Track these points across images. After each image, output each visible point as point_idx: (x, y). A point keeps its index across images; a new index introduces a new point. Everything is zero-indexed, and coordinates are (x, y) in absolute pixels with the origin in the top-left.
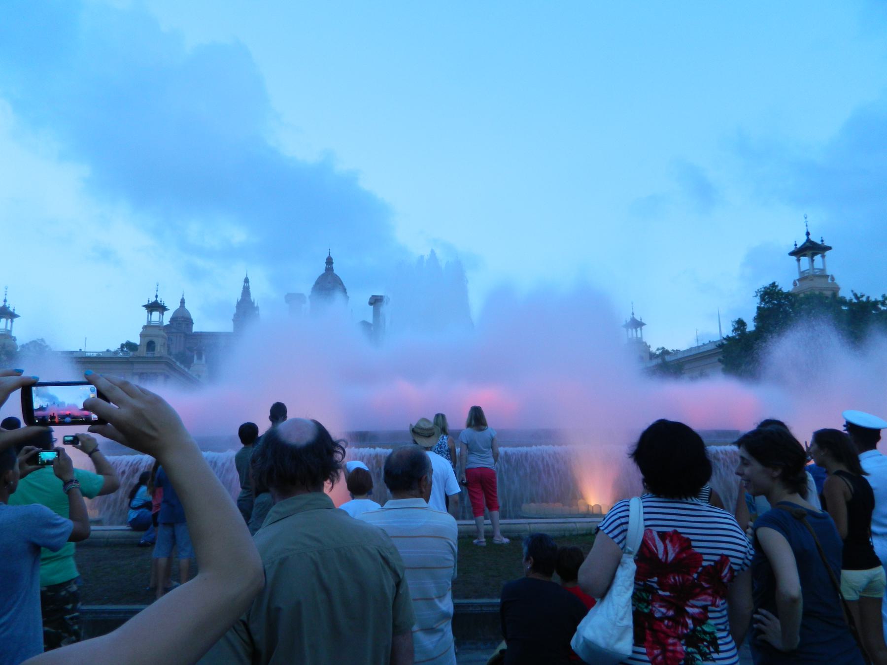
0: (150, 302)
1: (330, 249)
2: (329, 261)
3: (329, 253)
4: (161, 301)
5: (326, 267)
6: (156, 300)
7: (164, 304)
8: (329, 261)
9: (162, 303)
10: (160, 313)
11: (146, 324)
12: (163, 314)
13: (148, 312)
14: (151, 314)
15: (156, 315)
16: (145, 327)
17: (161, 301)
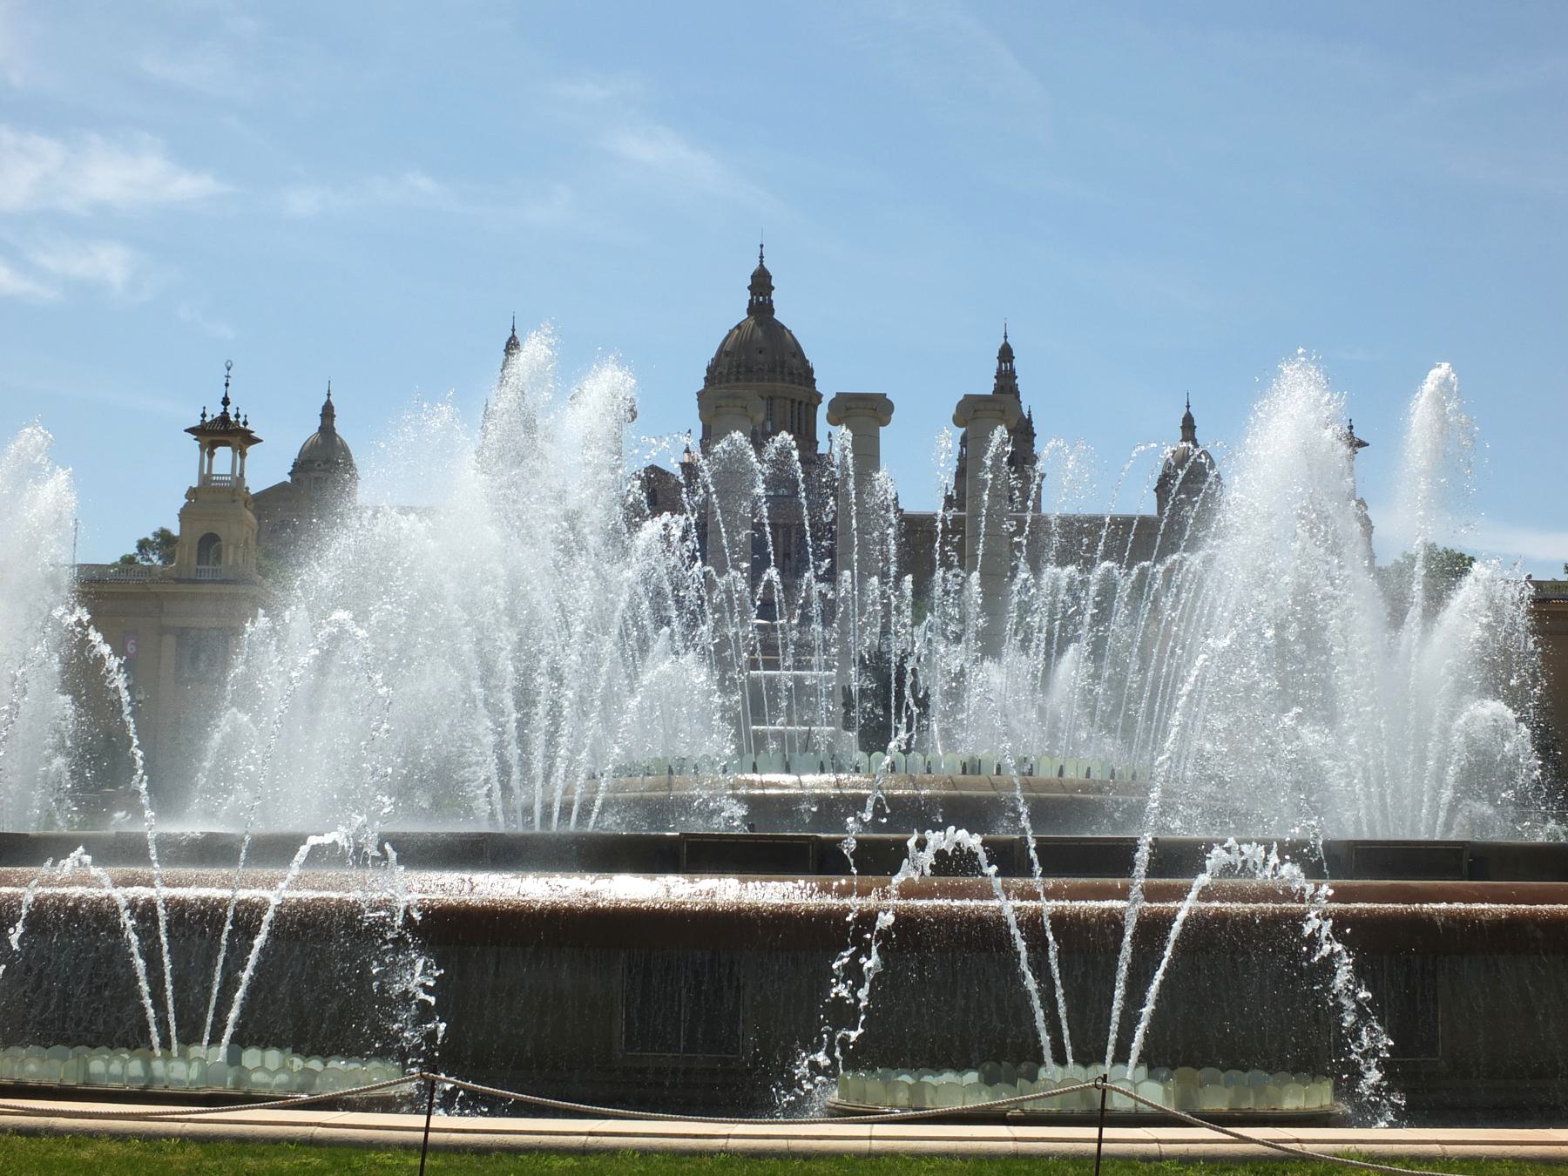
0: (208, 419)
1: (762, 246)
2: (761, 283)
3: (762, 257)
4: (237, 416)
5: (751, 302)
6: (225, 416)
7: (245, 423)
8: (761, 283)
9: (241, 420)
10: (234, 451)
11: (195, 485)
12: (243, 455)
13: (202, 448)
14: (211, 455)
15: (223, 458)
16: (192, 493)
17: (237, 416)
